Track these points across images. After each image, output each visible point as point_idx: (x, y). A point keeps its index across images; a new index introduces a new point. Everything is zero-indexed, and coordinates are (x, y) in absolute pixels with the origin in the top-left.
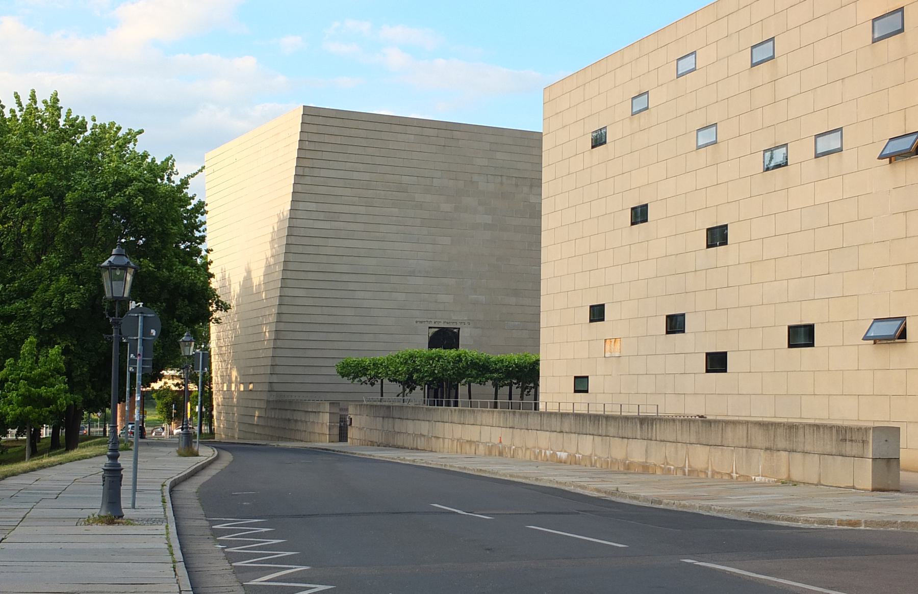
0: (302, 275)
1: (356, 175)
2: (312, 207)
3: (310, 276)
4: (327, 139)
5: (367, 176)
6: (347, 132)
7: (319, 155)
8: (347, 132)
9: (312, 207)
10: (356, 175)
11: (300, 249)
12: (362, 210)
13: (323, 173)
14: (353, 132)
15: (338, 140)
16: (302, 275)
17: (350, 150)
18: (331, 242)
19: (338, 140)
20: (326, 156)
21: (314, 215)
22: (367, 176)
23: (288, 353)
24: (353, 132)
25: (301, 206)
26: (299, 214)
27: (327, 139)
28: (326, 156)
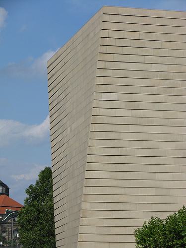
0: (106, 159)
1: (154, 68)
2: (114, 97)
3: (113, 159)
4: (127, 35)
5: (165, 68)
7: (119, 50)
9: (114, 97)
10: (154, 68)
11: (103, 135)
12: (161, 98)
16: (106, 159)
17: (149, 44)
18: (132, 129)
20: (125, 50)
21: (116, 104)
22: (165, 68)
23: (93, 230)
25: (104, 96)
27: (127, 35)
28: (125, 50)
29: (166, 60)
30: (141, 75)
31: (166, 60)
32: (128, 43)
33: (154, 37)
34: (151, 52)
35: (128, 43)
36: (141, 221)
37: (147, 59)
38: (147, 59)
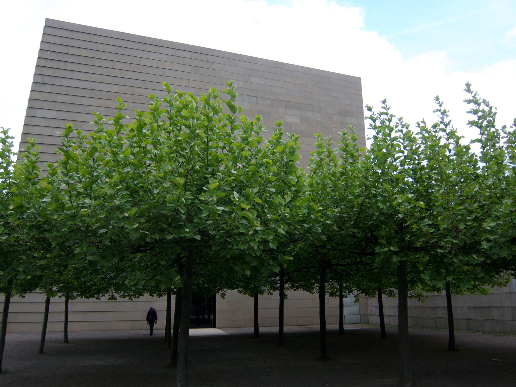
1: (102, 87)
4: (71, 51)
6: (95, 46)
8: (95, 46)
10: (102, 87)
13: (65, 82)
14: (101, 47)
15: (84, 53)
17: (97, 63)
19: (84, 53)
20: (69, 66)
24: (101, 47)
25: (39, 113)
26: (35, 121)
27: (71, 51)
28: (69, 66)
29: (117, 81)
30: (86, 93)
31: (117, 81)
32: (73, 59)
33: (103, 56)
34: (100, 71)
35: (73, 59)
36: (152, 306)
37: (95, 78)
38: (95, 78)
